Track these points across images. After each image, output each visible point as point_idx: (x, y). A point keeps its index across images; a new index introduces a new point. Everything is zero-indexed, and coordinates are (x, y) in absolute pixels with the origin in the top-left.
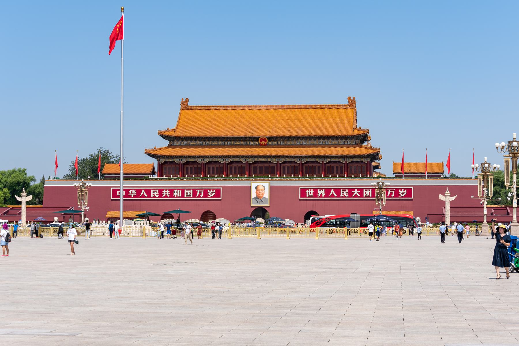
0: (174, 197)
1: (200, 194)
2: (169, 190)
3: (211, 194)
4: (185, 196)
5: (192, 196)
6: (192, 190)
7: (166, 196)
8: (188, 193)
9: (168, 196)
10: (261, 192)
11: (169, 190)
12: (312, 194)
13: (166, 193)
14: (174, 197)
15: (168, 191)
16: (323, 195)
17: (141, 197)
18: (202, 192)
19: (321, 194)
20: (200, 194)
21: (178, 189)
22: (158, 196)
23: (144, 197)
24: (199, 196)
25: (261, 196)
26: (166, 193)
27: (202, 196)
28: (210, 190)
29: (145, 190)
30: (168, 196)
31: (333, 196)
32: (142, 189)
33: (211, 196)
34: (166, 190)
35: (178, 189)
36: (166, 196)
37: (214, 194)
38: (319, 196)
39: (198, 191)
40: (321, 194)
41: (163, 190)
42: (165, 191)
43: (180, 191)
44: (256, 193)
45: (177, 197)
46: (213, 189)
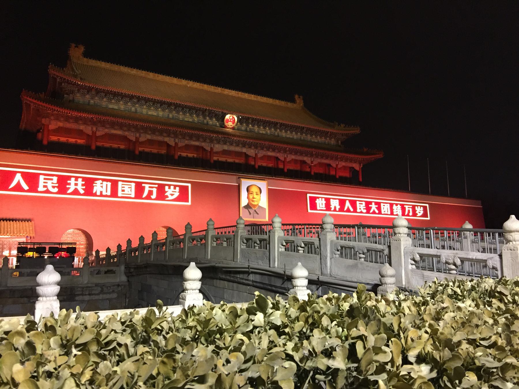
0: (95, 195)
1: (150, 193)
2: (84, 179)
3: (172, 195)
4: (120, 194)
5: (133, 195)
6: (133, 185)
7: (76, 192)
8: (126, 188)
9: (82, 192)
10: (255, 196)
11: (84, 179)
12: (324, 206)
13: (76, 184)
14: (95, 195)
15: (80, 182)
16: (338, 207)
17: (13, 189)
18: (155, 191)
19: (335, 207)
20: (150, 193)
21: (103, 180)
22: (56, 190)
23: (23, 190)
24: (148, 197)
25: (255, 203)
26: (76, 184)
27: (154, 196)
28: (169, 186)
29: (24, 175)
30: (82, 192)
31: (348, 210)
32: (16, 172)
33: (171, 197)
34: (77, 178)
35: (103, 180)
36: (76, 192)
37: (177, 194)
38: (332, 209)
39: (147, 187)
40: (335, 207)
41: (69, 178)
42: (72, 181)
43: (109, 184)
44: (248, 198)
45: (101, 195)
46: (175, 186)
